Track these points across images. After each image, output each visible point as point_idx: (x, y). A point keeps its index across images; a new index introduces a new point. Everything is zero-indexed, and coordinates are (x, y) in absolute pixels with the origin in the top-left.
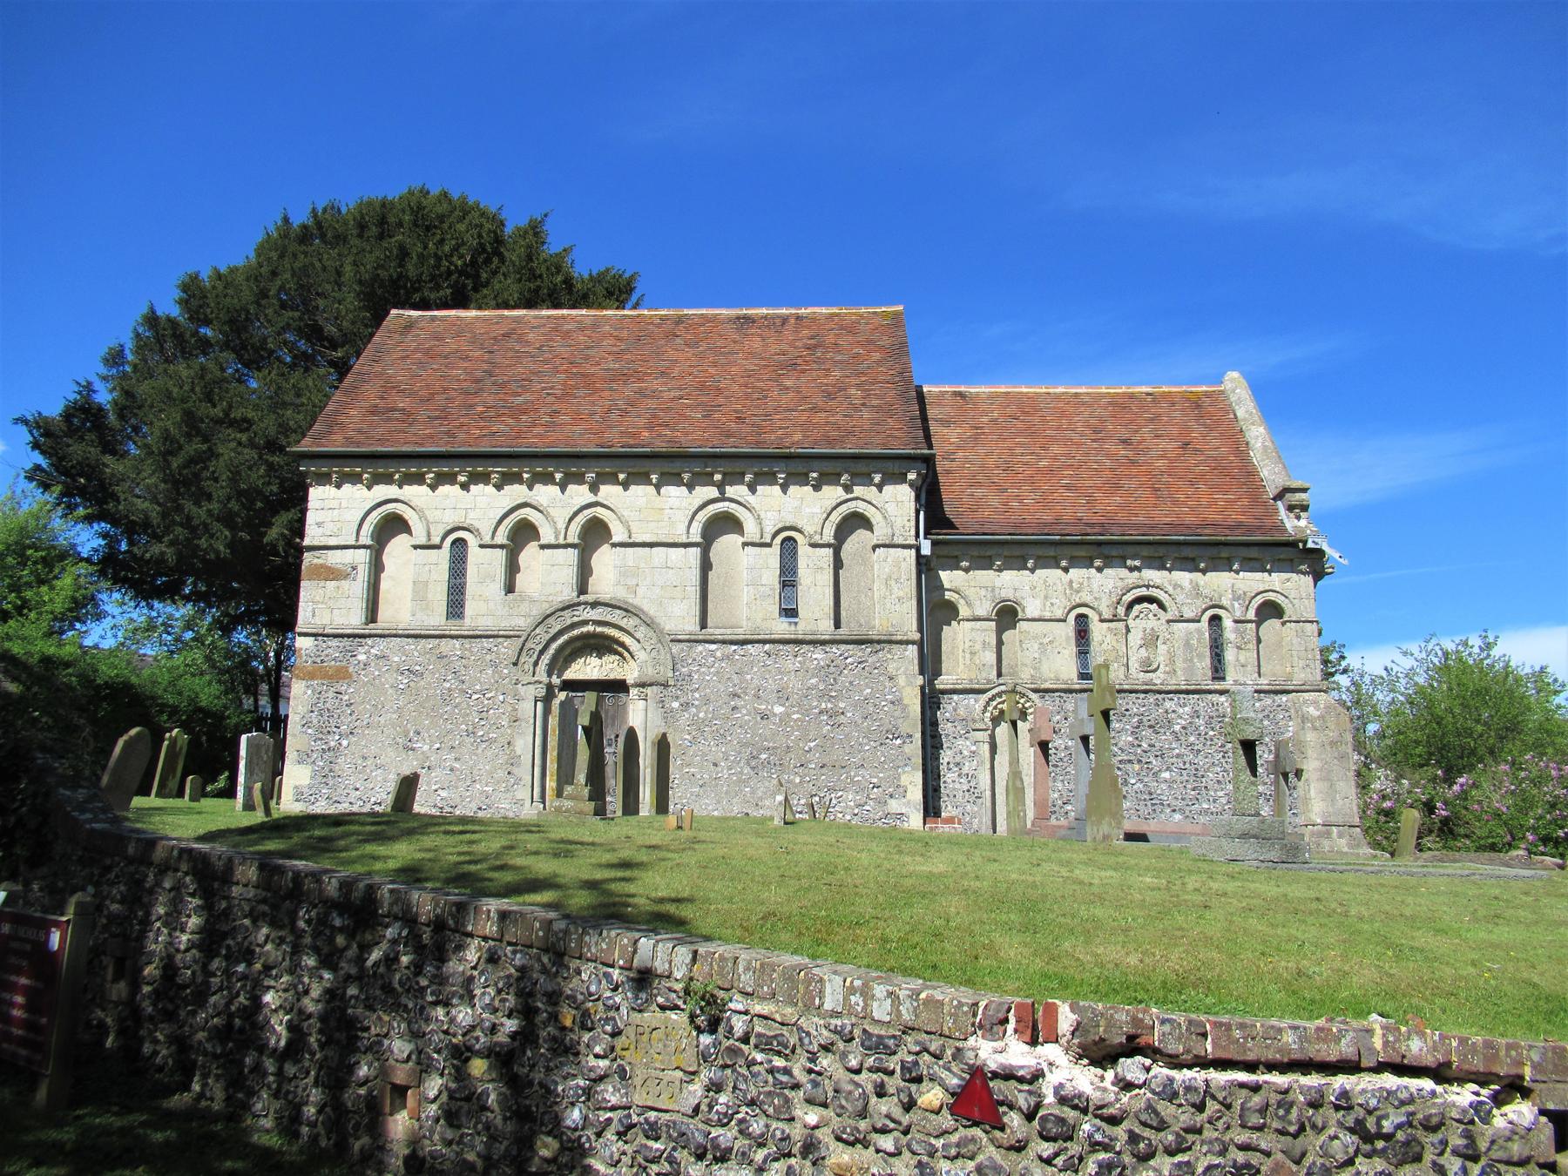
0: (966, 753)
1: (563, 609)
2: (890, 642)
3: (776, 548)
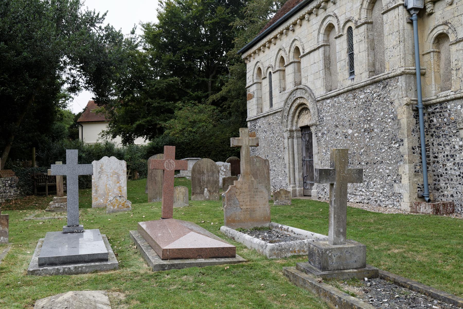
0: (457, 147)
1: (290, 95)
2: (390, 78)
3: (345, 38)
